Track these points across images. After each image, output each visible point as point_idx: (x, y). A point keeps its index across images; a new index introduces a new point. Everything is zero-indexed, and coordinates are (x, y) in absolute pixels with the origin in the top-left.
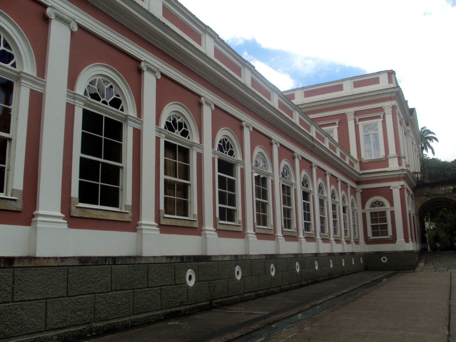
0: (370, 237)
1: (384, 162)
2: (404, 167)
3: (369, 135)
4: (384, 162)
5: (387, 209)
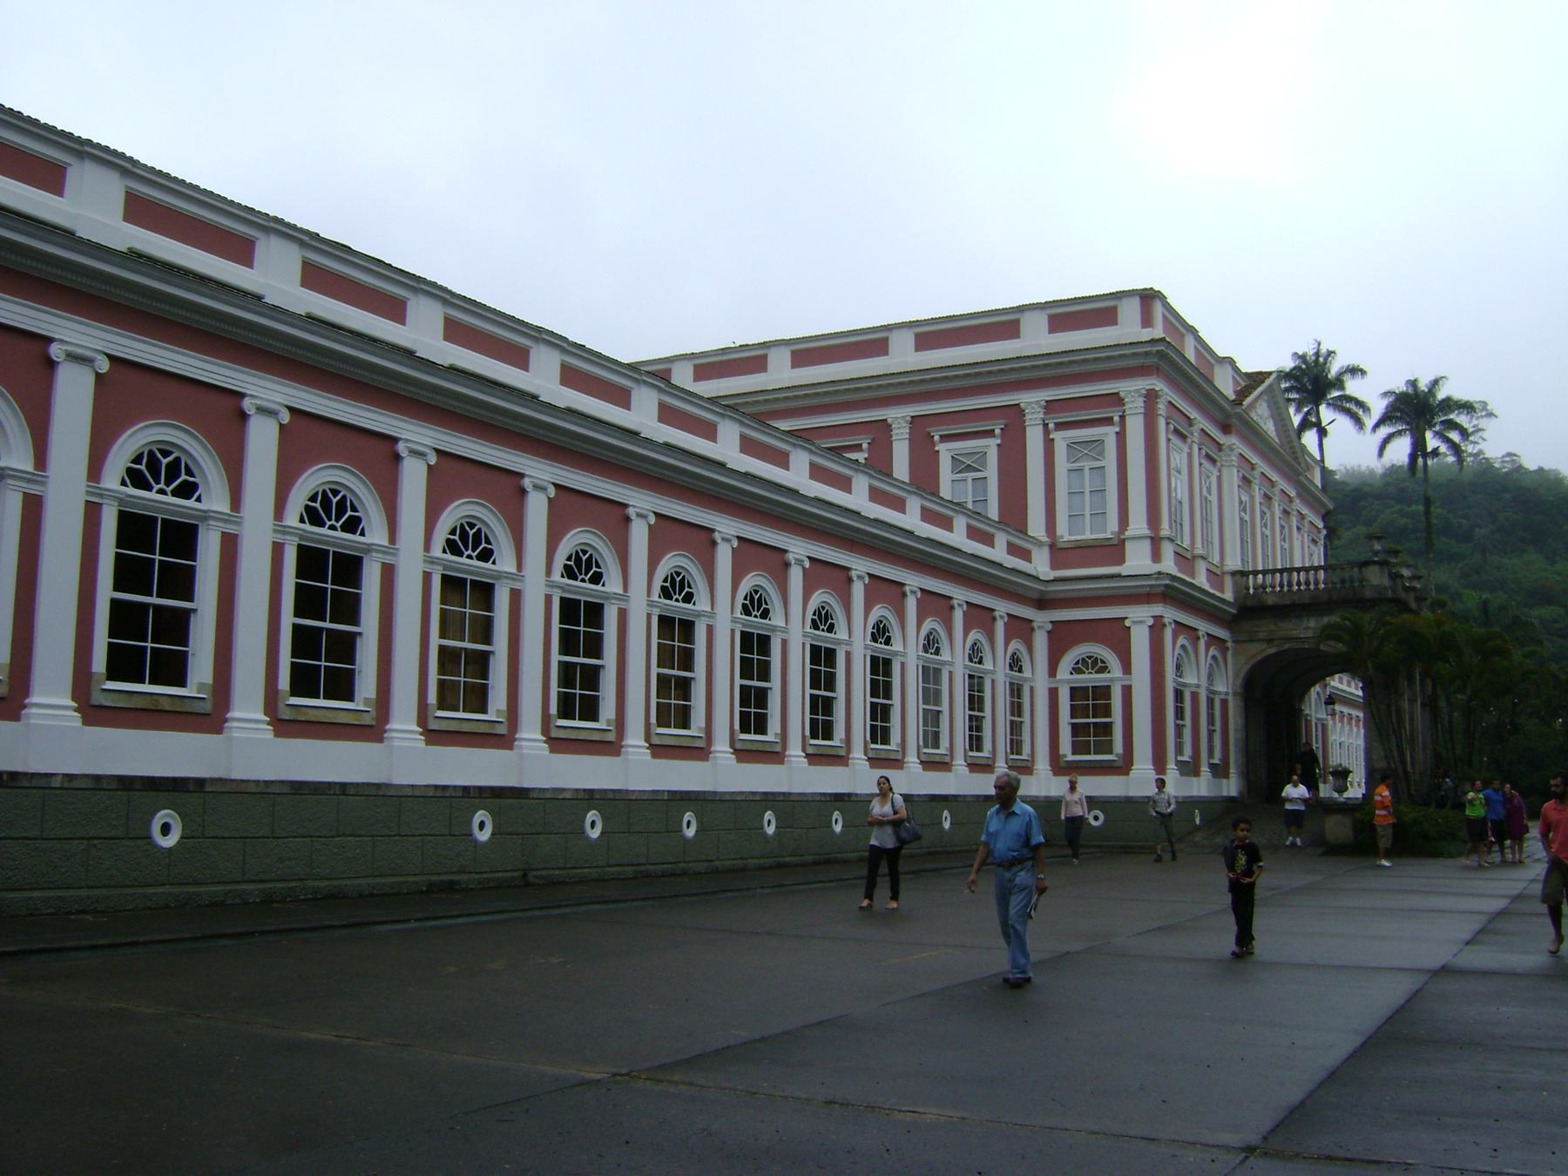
0: (1065, 756)
1: (1114, 550)
2: (1168, 565)
3: (1080, 470)
4: (1114, 550)
5: (1112, 680)
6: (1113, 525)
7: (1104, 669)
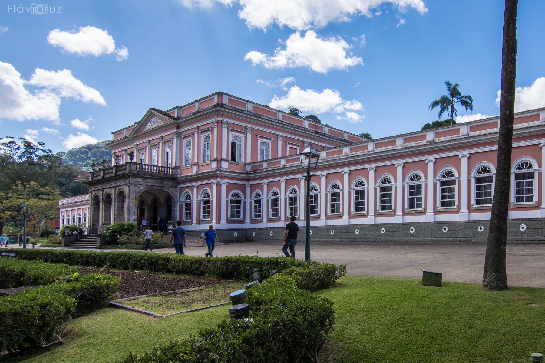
5: (242, 199)
6: (243, 160)
7: (239, 197)
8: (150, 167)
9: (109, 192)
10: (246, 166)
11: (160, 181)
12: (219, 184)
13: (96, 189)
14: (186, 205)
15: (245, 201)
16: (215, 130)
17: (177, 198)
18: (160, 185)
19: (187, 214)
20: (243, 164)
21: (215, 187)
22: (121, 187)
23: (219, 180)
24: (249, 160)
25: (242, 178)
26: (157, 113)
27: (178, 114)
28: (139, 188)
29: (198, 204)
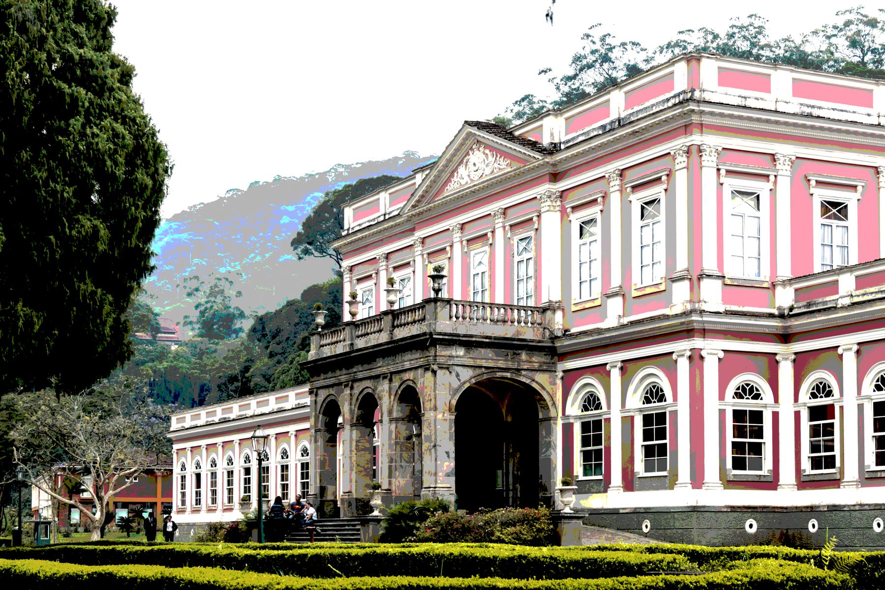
5: (765, 406)
7: (757, 397)
8: (523, 313)
9: (370, 391)
10: (779, 289)
11: (510, 352)
12: (696, 358)
13: (332, 381)
14: (585, 427)
15: (776, 410)
16: (681, 178)
17: (554, 404)
18: (510, 365)
19: (587, 456)
20: (766, 285)
21: (683, 366)
22: (407, 376)
23: (698, 342)
24: (785, 271)
25: (767, 331)
26: (487, 136)
27: (552, 134)
28: (458, 375)
29: (628, 422)
